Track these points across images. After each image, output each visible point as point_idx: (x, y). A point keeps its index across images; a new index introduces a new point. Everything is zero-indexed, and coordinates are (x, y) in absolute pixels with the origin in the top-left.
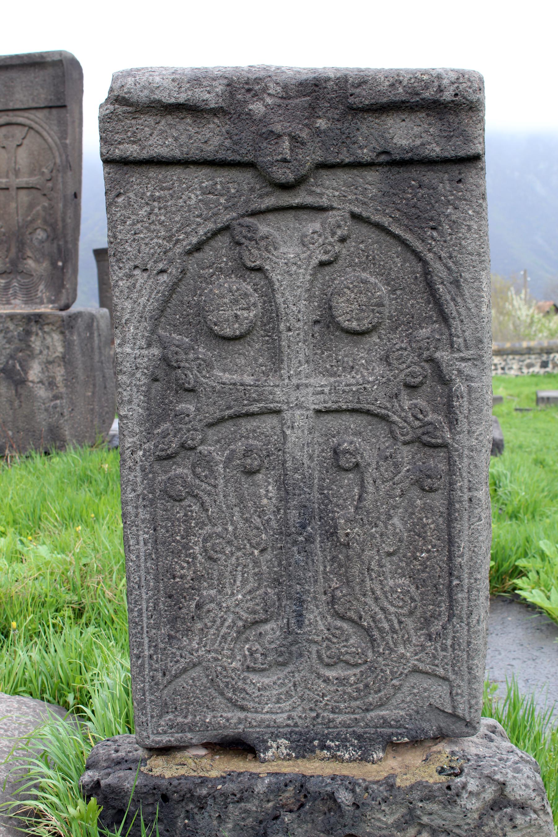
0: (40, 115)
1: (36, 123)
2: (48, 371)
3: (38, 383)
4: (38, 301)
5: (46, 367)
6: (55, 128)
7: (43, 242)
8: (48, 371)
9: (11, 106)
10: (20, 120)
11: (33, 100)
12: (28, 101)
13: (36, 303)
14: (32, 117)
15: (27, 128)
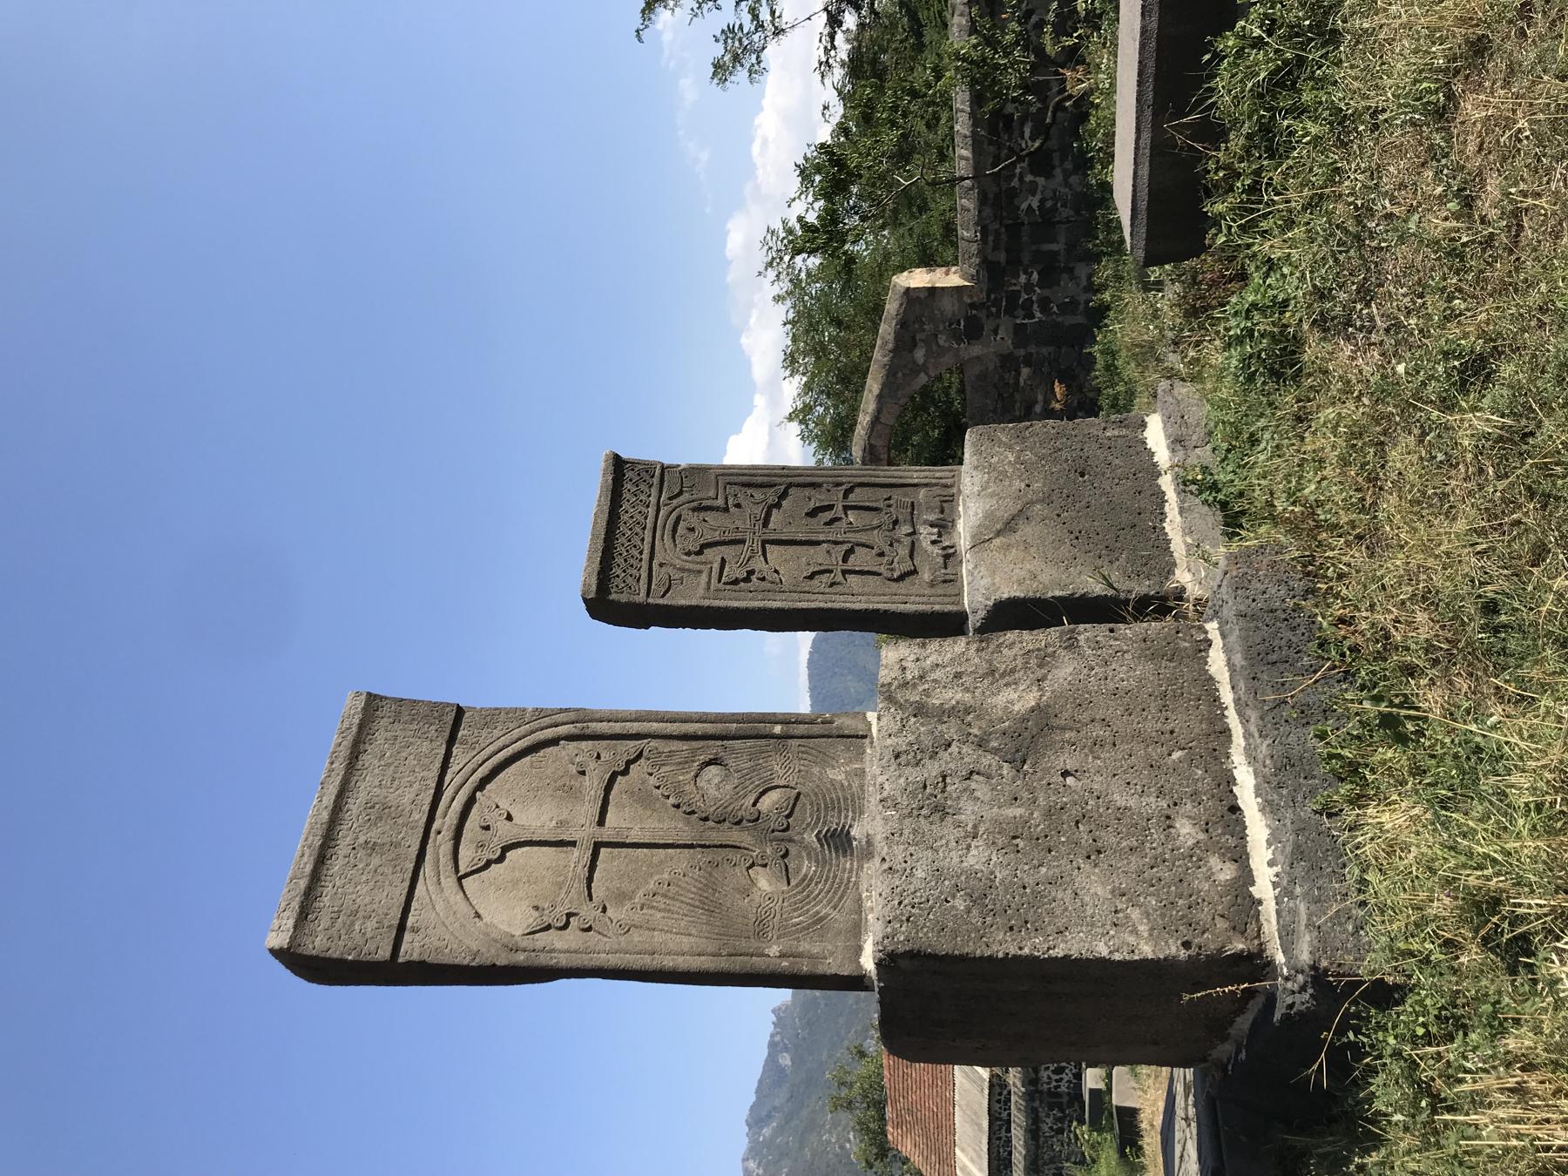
0: (460, 757)
1: (474, 771)
2: (1013, 671)
3: (1040, 689)
4: (855, 785)
5: (1003, 675)
6: (497, 733)
7: (726, 776)
8: (1013, 671)
9: (420, 818)
10: (457, 805)
11: (426, 768)
12: (424, 779)
13: (862, 787)
14: (458, 780)
15: (478, 794)
